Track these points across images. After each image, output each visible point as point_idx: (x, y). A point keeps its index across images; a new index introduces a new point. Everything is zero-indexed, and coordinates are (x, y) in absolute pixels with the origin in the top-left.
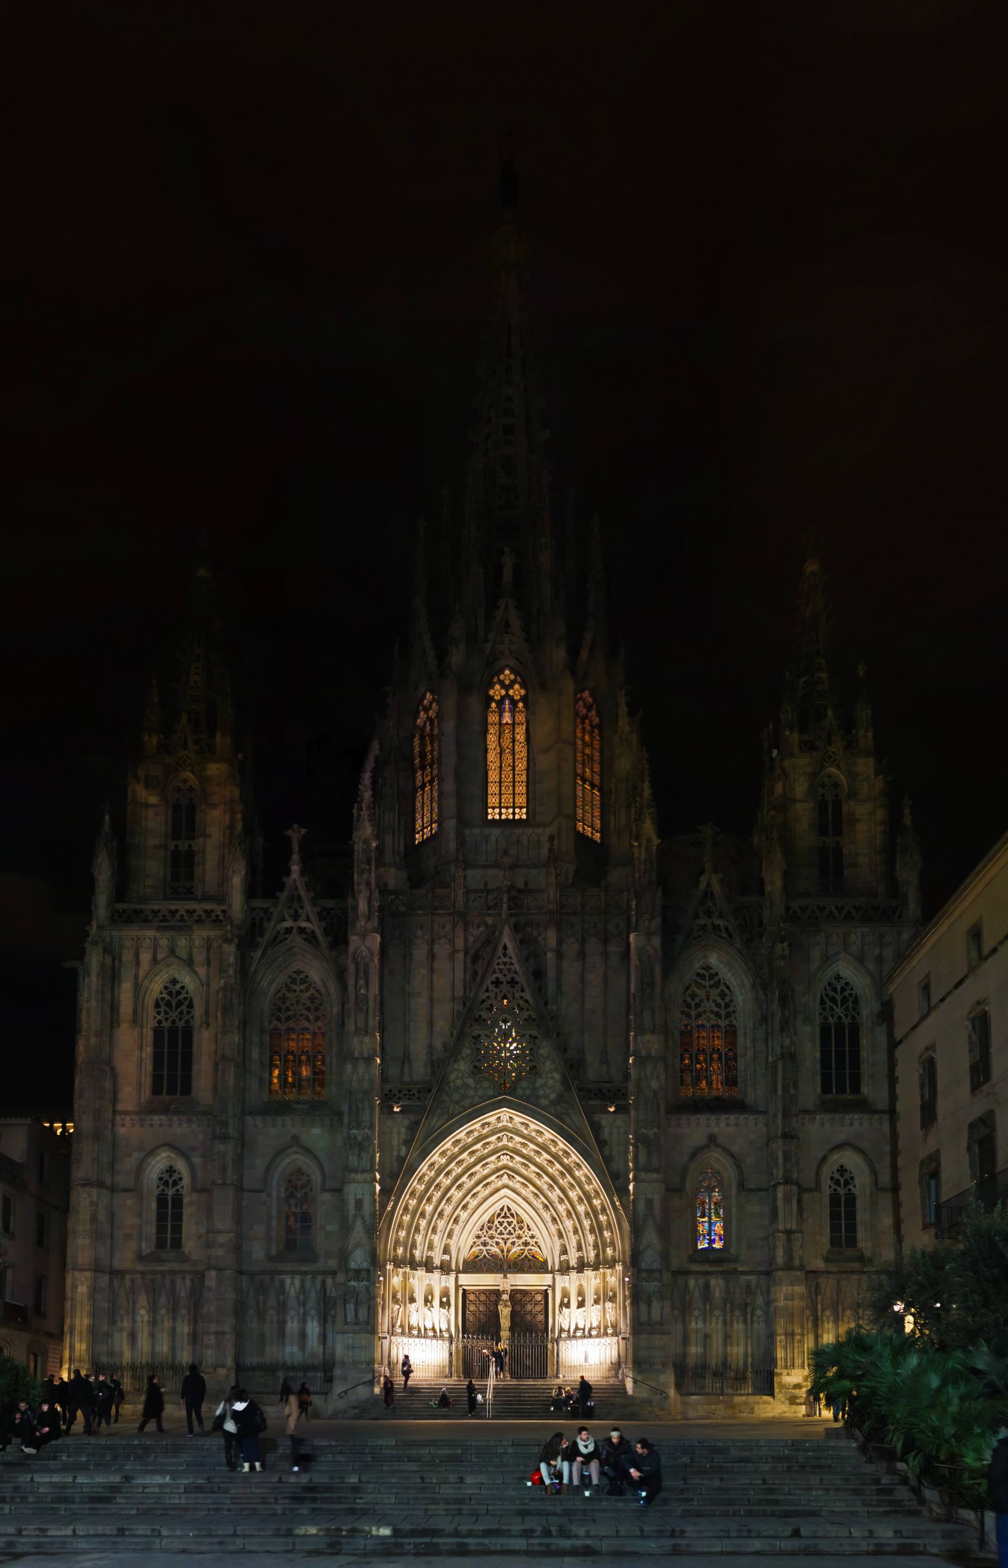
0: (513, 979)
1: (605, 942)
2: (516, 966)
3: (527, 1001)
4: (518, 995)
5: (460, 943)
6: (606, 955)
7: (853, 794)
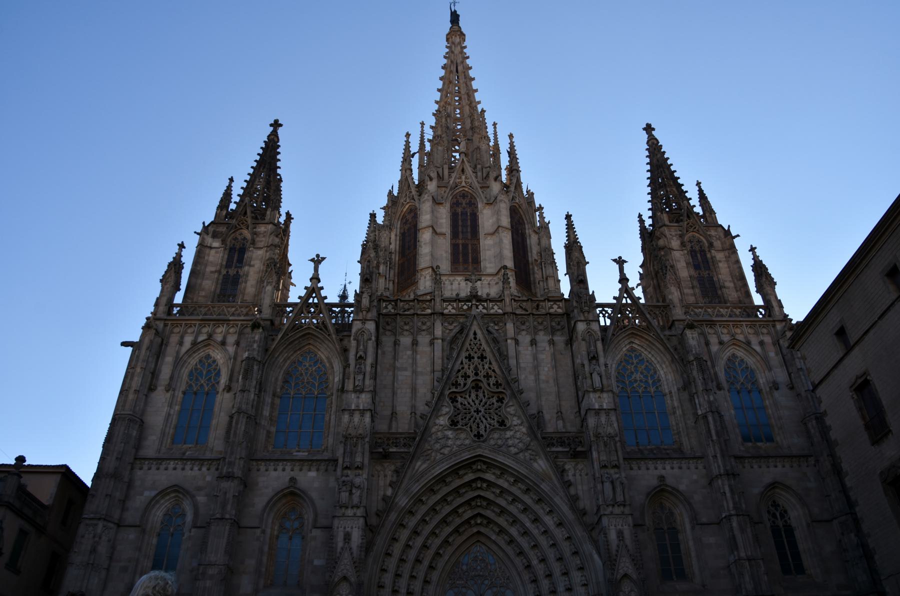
0: (482, 355)
1: (553, 334)
2: (484, 346)
3: (494, 371)
4: (486, 366)
5: (438, 332)
6: (552, 342)
7: (711, 245)
